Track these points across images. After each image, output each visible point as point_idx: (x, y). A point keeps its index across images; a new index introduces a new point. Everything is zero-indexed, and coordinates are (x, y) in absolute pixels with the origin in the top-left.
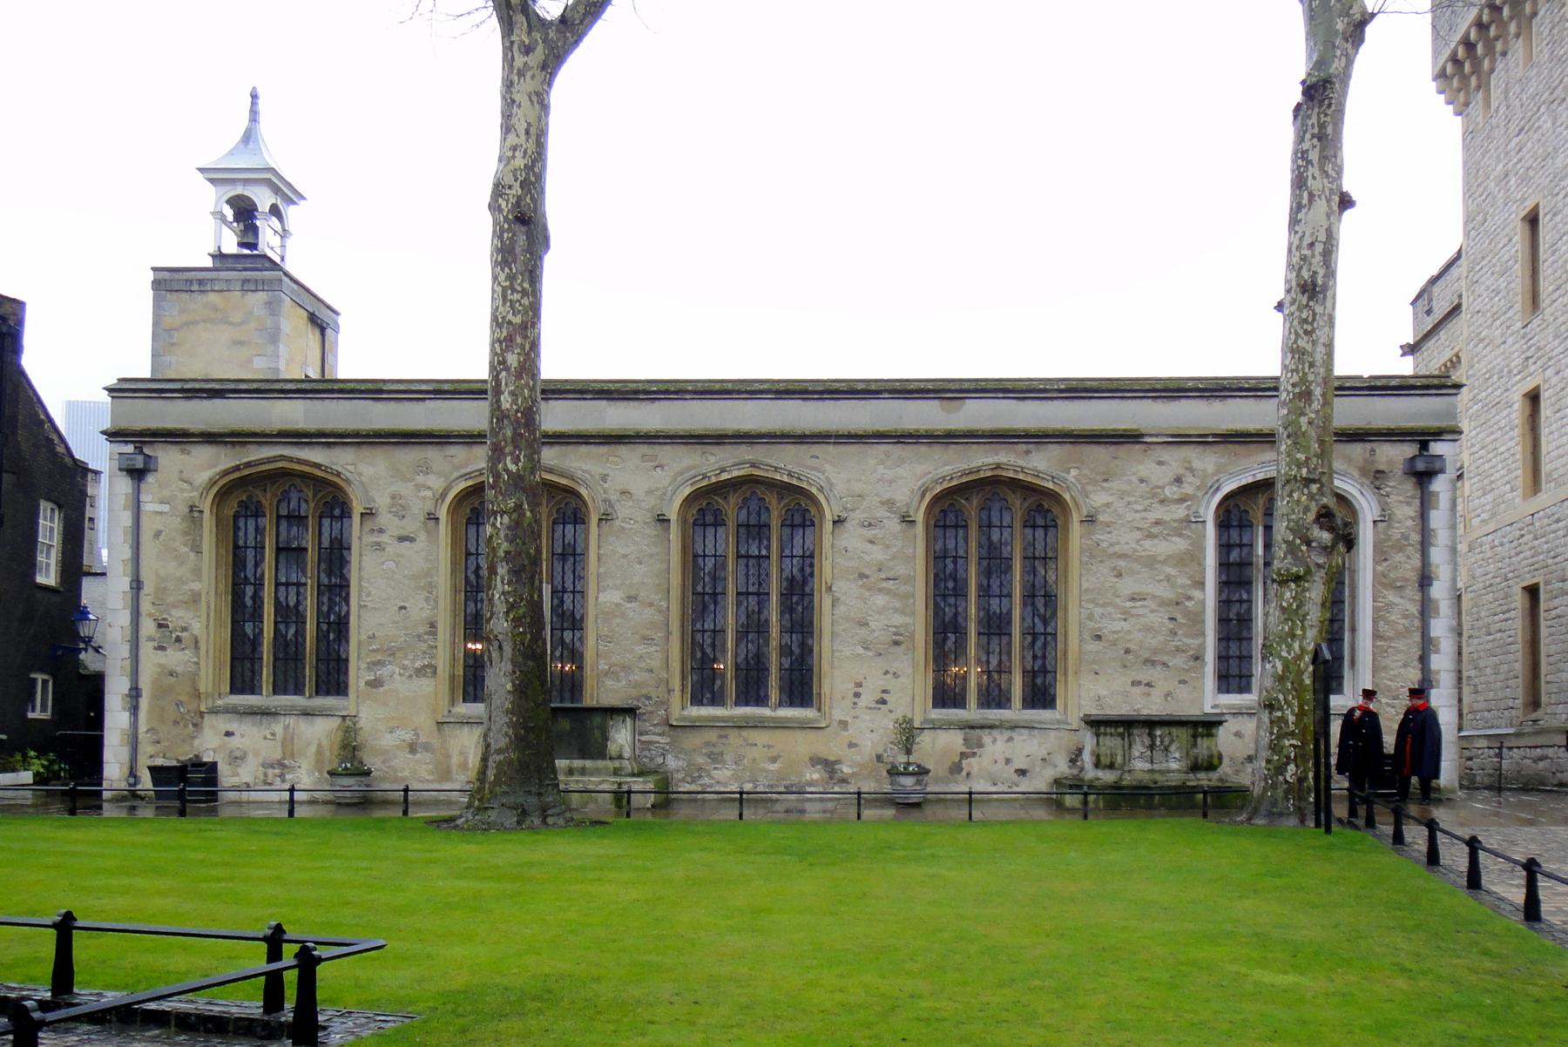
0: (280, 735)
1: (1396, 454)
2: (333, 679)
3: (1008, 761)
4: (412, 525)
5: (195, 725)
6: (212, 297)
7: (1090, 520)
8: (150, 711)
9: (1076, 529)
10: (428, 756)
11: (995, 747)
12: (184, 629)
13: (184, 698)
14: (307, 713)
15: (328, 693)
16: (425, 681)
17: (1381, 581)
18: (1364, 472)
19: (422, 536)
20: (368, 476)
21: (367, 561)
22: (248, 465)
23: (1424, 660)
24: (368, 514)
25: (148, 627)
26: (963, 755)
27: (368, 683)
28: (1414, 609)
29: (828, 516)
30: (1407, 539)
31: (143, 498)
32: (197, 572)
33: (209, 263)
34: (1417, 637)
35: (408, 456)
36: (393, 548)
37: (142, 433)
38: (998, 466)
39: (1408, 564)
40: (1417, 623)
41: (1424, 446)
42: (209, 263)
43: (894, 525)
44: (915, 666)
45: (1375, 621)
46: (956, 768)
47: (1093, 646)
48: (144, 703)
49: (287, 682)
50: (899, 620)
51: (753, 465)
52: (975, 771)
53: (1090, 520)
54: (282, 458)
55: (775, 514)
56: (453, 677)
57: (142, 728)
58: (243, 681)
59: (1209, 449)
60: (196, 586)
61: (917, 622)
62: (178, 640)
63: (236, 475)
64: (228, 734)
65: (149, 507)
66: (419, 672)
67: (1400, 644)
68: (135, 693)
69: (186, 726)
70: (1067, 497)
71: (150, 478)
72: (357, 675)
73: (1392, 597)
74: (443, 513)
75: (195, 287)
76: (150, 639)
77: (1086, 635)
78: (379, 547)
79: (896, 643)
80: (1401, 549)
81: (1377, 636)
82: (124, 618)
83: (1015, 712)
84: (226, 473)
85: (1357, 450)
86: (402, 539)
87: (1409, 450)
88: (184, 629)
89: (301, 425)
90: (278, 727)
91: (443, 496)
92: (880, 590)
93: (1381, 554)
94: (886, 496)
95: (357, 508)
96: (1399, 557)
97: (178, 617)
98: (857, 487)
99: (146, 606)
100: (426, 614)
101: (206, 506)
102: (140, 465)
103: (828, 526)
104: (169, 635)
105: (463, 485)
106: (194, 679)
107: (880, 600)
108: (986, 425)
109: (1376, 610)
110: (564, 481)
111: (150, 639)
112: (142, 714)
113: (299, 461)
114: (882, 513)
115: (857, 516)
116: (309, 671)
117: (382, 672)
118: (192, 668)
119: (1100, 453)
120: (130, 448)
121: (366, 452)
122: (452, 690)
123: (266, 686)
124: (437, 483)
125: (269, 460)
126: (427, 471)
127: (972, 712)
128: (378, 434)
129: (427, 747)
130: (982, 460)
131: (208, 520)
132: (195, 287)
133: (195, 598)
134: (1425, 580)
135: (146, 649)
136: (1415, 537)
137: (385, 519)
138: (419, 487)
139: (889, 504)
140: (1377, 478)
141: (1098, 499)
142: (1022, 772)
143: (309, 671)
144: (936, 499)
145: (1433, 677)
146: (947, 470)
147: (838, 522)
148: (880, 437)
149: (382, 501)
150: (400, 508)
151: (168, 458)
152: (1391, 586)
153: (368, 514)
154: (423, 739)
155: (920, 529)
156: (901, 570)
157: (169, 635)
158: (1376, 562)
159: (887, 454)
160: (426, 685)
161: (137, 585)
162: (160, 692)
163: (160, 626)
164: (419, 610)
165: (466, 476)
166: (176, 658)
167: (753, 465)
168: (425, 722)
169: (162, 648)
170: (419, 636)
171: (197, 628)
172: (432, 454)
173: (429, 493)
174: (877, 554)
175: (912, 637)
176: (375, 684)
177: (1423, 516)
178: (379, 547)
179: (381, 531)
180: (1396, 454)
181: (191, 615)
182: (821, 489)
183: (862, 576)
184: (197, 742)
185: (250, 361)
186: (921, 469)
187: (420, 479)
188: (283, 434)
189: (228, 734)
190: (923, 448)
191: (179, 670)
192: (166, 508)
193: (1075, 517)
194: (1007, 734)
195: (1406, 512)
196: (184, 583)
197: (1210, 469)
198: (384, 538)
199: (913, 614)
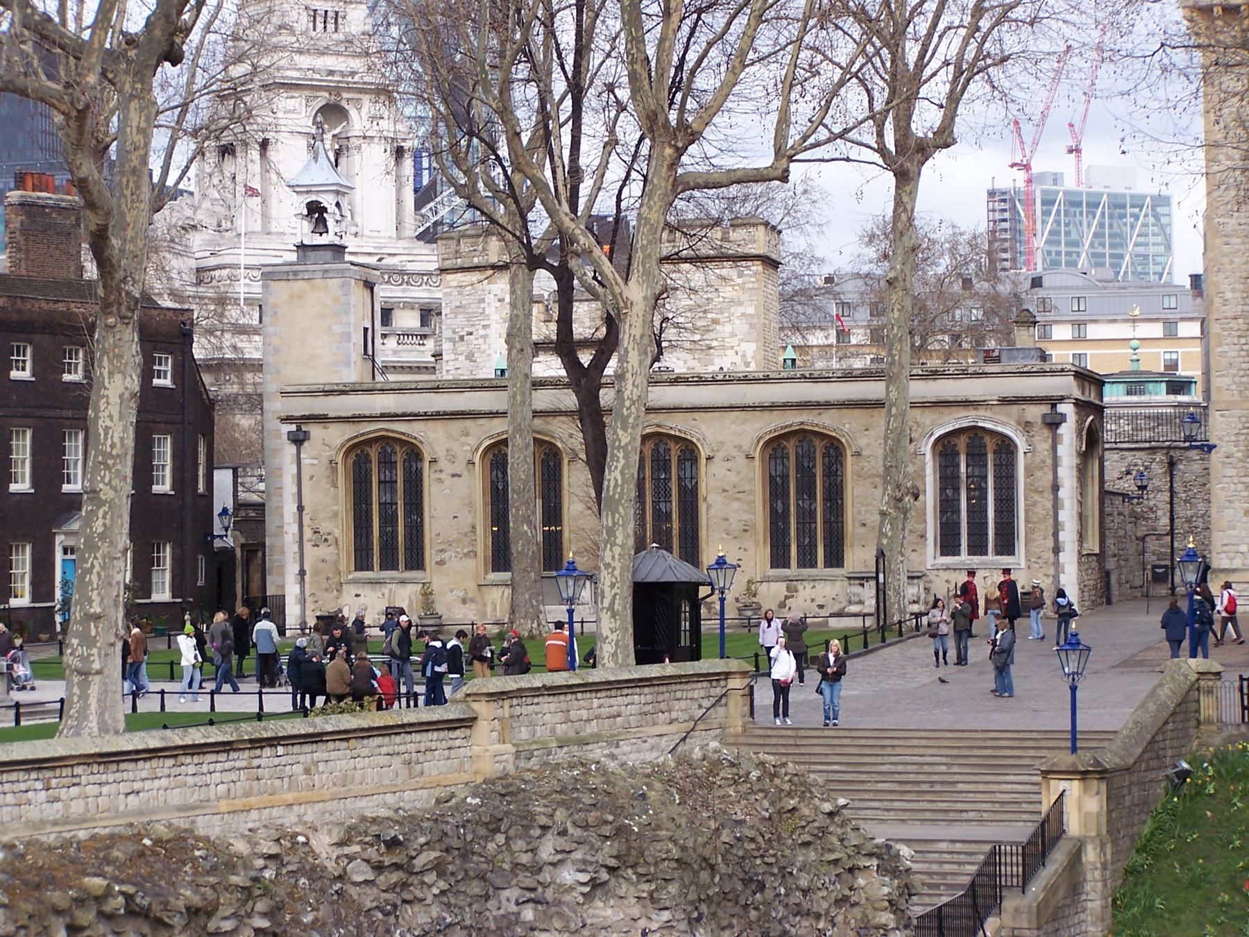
1: (1036, 412)
2: (416, 561)
3: (813, 600)
4: (460, 467)
6: (300, 284)
7: (858, 454)
8: (311, 584)
9: (849, 460)
10: (473, 606)
11: (805, 592)
13: (331, 575)
14: (403, 582)
15: (412, 569)
16: (470, 561)
17: (1029, 488)
18: (1019, 423)
19: (465, 473)
20: (434, 440)
21: (433, 489)
22: (363, 434)
23: (1056, 535)
24: (434, 461)
25: (308, 533)
26: (787, 597)
27: (437, 563)
28: (1049, 505)
29: (703, 455)
30: (1044, 462)
31: (302, 456)
32: (336, 498)
33: (293, 257)
34: (1051, 521)
35: (457, 425)
36: (449, 481)
37: (303, 417)
38: (802, 423)
39: (1046, 479)
40: (1051, 513)
41: (1054, 406)
42: (293, 257)
43: (742, 461)
44: (757, 543)
45: (1026, 512)
46: (782, 605)
47: (863, 530)
48: (307, 578)
49: (389, 563)
50: (746, 517)
51: (658, 426)
52: (793, 606)
53: (858, 454)
54: (382, 429)
55: (673, 453)
56: (485, 558)
57: (307, 593)
58: (363, 563)
59: (927, 411)
60: (335, 508)
61: (759, 518)
62: (326, 540)
63: (356, 441)
64: (357, 596)
65: (306, 461)
66: (467, 555)
67: (1042, 526)
68: (302, 573)
70: (843, 441)
71: (306, 444)
72: (430, 556)
73: (1036, 497)
74: (477, 459)
75: (291, 277)
76: (310, 540)
77: (857, 524)
78: (440, 481)
79: (745, 531)
80: (1041, 469)
81: (1027, 521)
82: (294, 529)
83: (820, 570)
84: (351, 439)
85: (1015, 409)
86: (453, 476)
87: (1045, 409)
88: (329, 534)
89: (393, 410)
91: (477, 449)
92: (736, 499)
93: (1029, 473)
94: (737, 442)
95: (427, 458)
96: (1039, 474)
97: (325, 527)
98: (720, 438)
99: (306, 521)
100: (470, 520)
101: (339, 459)
102: (301, 437)
103: (703, 461)
104: (321, 538)
105: (488, 443)
106: (336, 563)
107: (736, 505)
108: (794, 399)
109: (1026, 505)
110: (547, 439)
111: (310, 540)
112: (307, 586)
114: (735, 453)
115: (719, 456)
116: (401, 557)
117: (446, 556)
118: (335, 557)
119: (857, 413)
120: (293, 428)
121: (431, 424)
122: (485, 565)
123: (376, 566)
124: (472, 441)
125: (375, 431)
126: (467, 435)
127: (793, 571)
128: (438, 414)
129: (472, 600)
130: (794, 419)
131: (340, 468)
132: (291, 277)
133: (336, 515)
134: (1056, 488)
135: (308, 546)
136: (1049, 461)
137: (443, 464)
138: (463, 444)
139: (739, 447)
140: (1027, 426)
141: (862, 442)
142: (821, 607)
143: (401, 557)
144: (767, 443)
145: (1061, 545)
146: (772, 426)
147: (709, 458)
148: (732, 408)
149: (441, 454)
150: (452, 459)
151: (315, 430)
152: (1036, 491)
153: (434, 461)
154: (470, 595)
155: (757, 462)
156: (747, 487)
157: (321, 538)
158: (1026, 477)
160: (470, 564)
161: (301, 508)
162: (316, 572)
164: (465, 520)
165: (490, 437)
166: (325, 551)
167: (658, 426)
168: (471, 585)
170: (466, 534)
171: (337, 532)
172: (469, 423)
173: (468, 448)
174: (733, 478)
175: (754, 526)
176: (441, 563)
177: (1054, 448)
178: (440, 481)
179: (441, 471)
180: (1036, 412)
182: (698, 439)
183: (724, 491)
185: (330, 328)
186: (757, 425)
187: (463, 439)
189: (357, 596)
190: (758, 413)
192: (315, 462)
193: (849, 453)
194: (812, 584)
195: (1044, 446)
197: (928, 422)
198: (443, 476)
199: (754, 513)
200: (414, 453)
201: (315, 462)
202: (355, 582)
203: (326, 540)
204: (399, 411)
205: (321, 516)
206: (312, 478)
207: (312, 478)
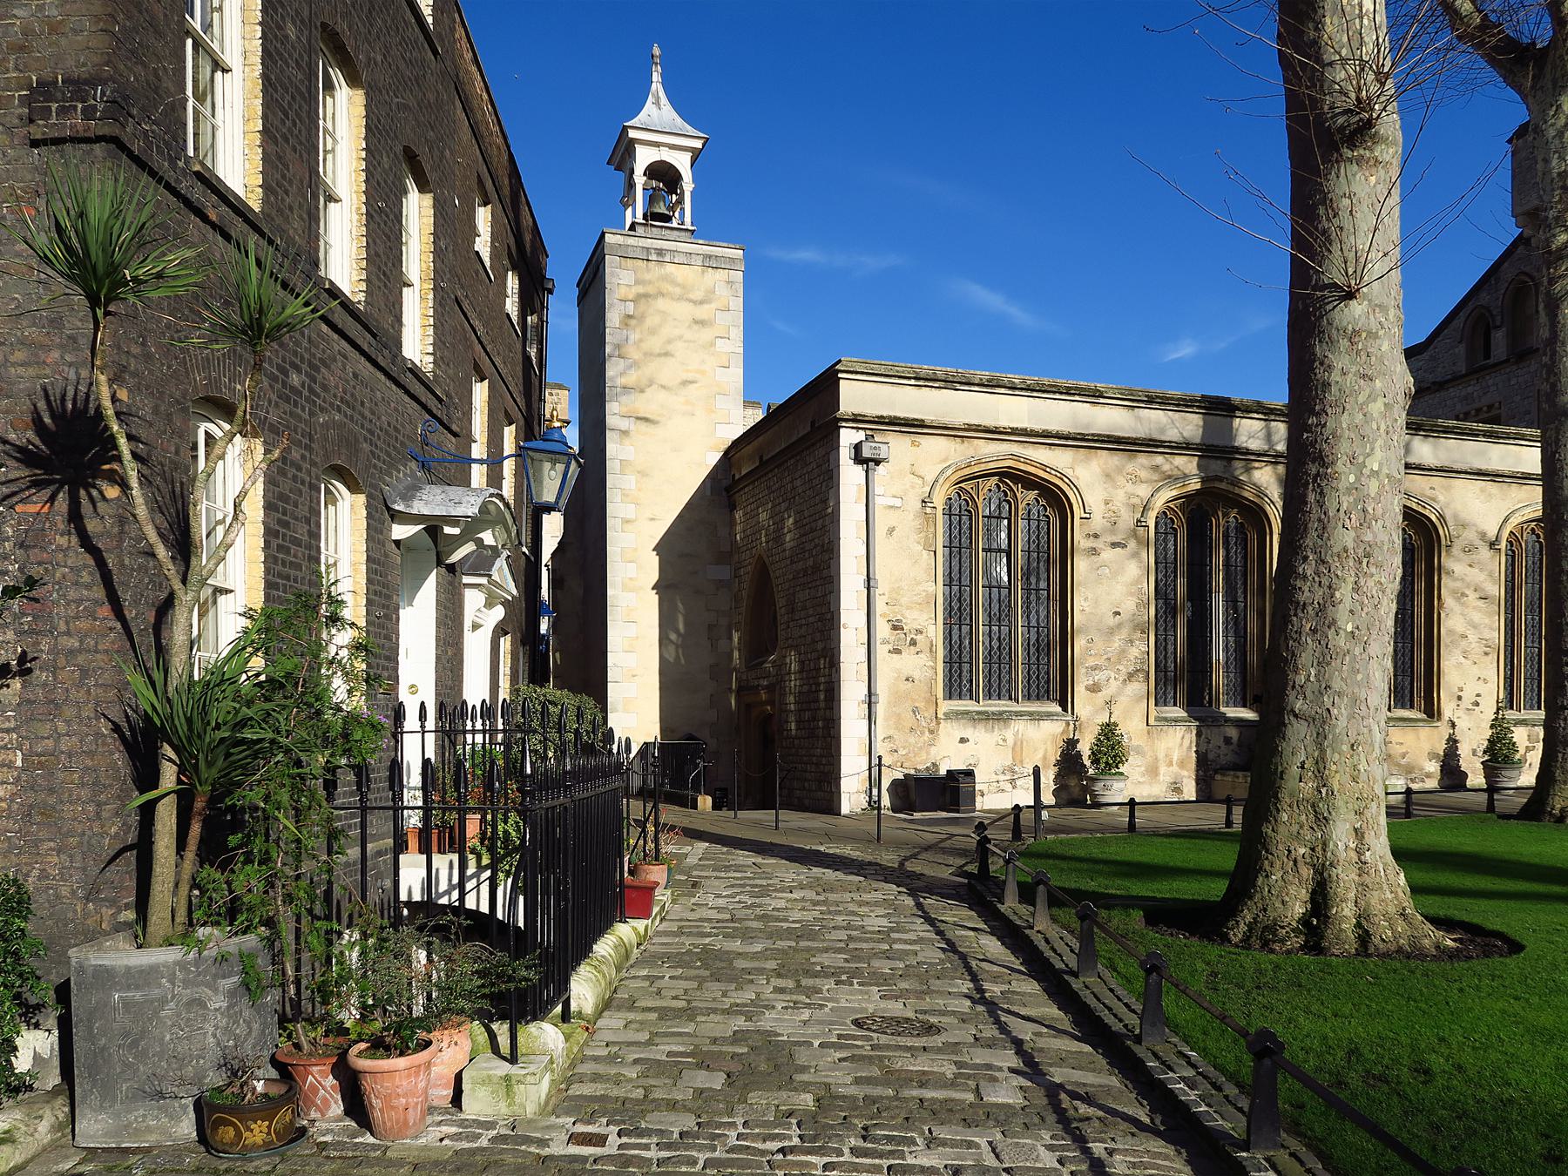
0: (1010, 742)
5: (931, 732)
8: (886, 719)
12: (919, 632)
13: (921, 705)
25: (882, 630)
58: (957, 685)
64: (963, 740)
68: (870, 702)
69: (922, 733)
76: (885, 642)
86: (1114, 545)
88: (919, 632)
90: (1009, 734)
99: (880, 606)
111: (885, 642)
113: (1028, 461)
117: (1100, 676)
120: (861, 436)
135: (881, 651)
159: (1482, 490)
162: (897, 698)
163: (895, 628)
169: (897, 651)
181: (925, 616)
184: (933, 750)
188: (1015, 431)
189: (963, 740)
191: (916, 675)
196: (919, 583)
200: (1055, 499)
201: (898, 503)
202: (953, 716)
203: (913, 643)
204: (1038, 427)
205: (904, 600)
206: (891, 531)
207: (891, 531)
